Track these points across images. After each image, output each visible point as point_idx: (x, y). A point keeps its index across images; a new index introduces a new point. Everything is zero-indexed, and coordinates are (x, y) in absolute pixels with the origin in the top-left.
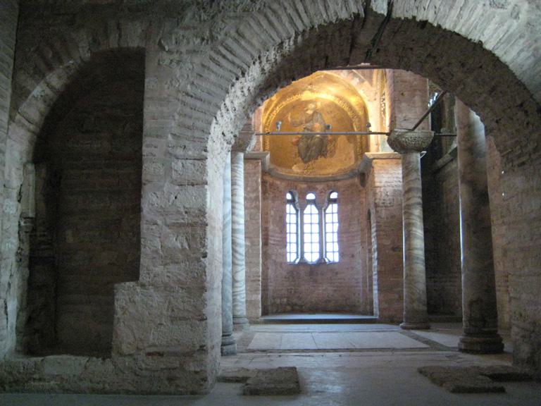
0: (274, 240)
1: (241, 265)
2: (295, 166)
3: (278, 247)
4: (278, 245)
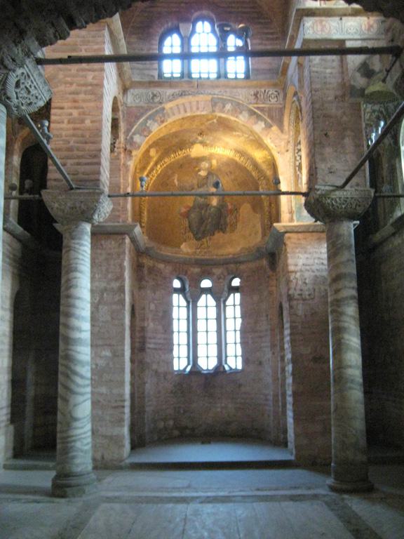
0: (155, 344)
1: (82, 394)
2: (184, 244)
3: (160, 352)
4: (160, 349)
